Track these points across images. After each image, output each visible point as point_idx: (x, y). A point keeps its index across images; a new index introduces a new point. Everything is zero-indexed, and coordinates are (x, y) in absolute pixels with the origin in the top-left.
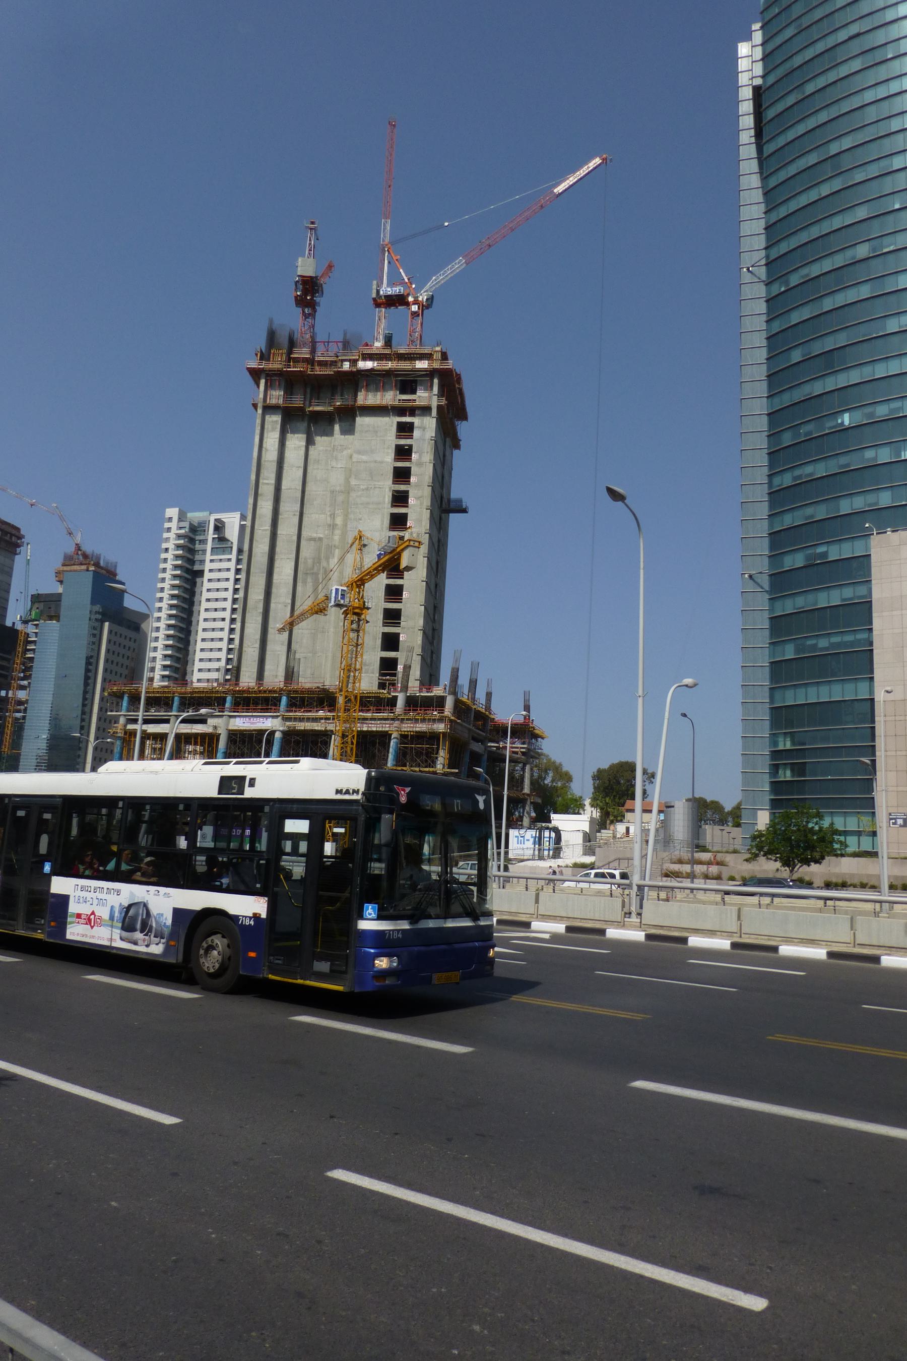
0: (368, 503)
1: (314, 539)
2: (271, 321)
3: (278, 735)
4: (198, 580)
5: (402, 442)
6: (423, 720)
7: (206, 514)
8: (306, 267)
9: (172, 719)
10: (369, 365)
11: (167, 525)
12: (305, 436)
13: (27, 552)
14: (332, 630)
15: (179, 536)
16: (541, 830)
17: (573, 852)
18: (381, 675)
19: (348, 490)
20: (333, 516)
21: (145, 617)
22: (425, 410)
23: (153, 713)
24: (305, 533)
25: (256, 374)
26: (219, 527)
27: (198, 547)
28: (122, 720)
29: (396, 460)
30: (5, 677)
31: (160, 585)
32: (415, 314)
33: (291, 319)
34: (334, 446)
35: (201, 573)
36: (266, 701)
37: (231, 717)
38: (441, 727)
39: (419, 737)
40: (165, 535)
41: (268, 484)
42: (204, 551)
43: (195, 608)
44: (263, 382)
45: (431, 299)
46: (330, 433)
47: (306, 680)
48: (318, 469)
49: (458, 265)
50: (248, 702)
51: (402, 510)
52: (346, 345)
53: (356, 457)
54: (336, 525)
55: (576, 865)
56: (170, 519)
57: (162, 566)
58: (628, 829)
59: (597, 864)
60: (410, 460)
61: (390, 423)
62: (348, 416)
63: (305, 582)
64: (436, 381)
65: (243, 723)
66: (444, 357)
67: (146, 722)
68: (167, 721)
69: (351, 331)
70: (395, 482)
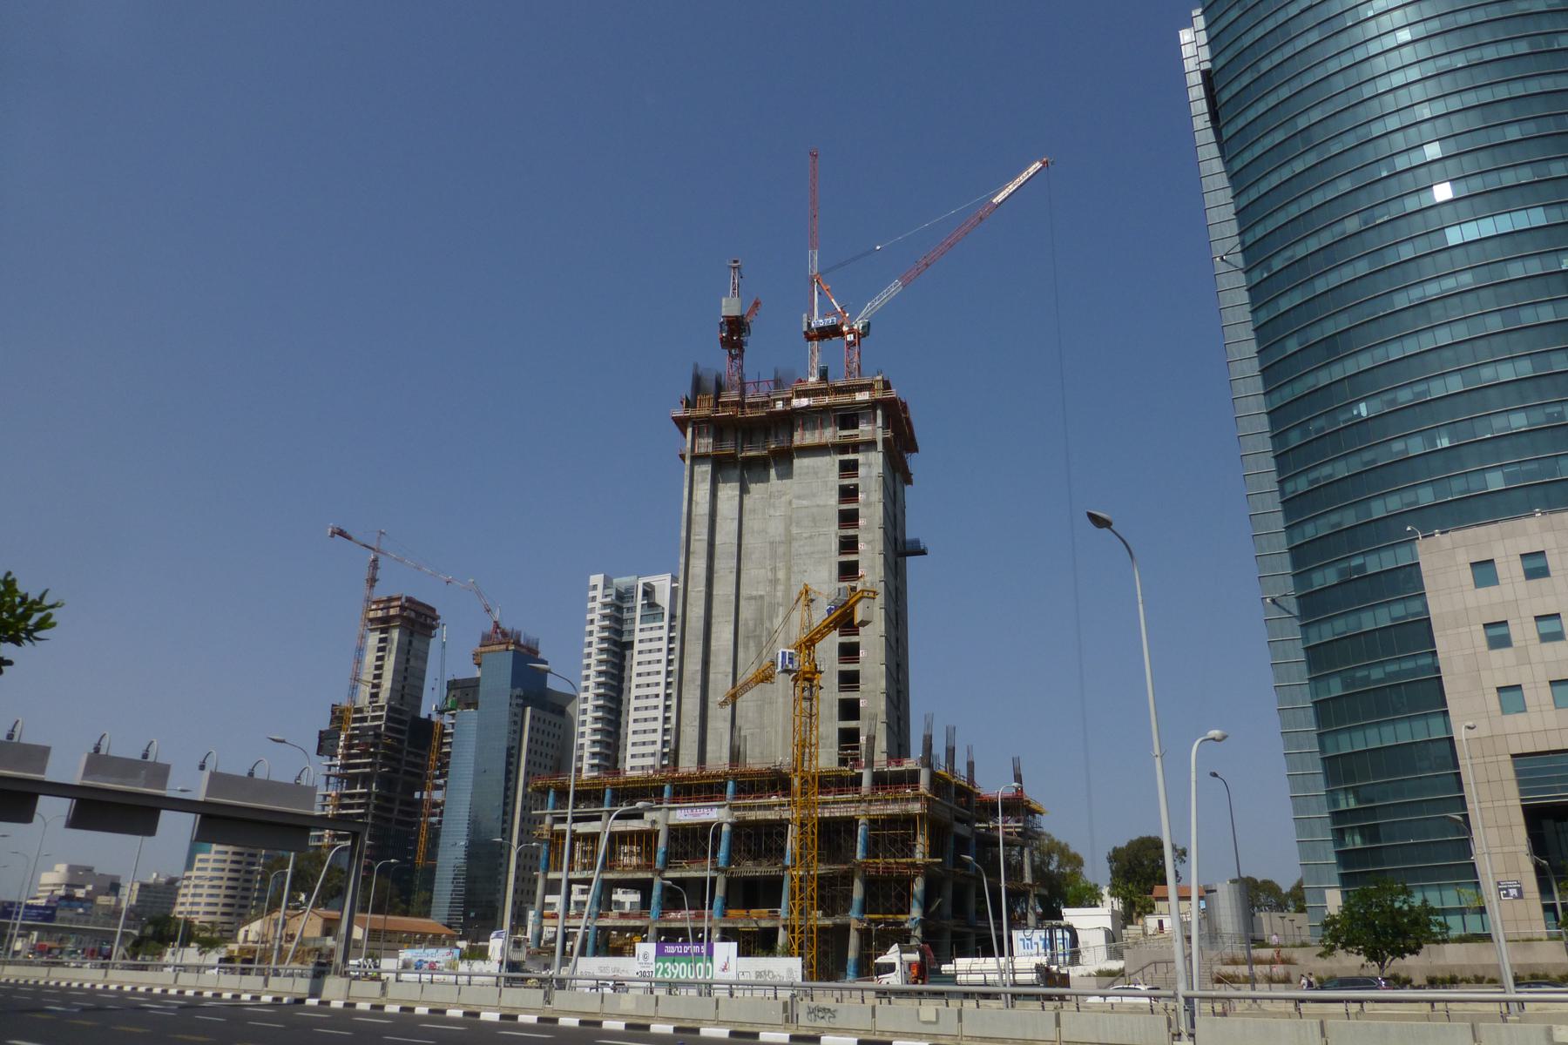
1: (754, 598)
2: (696, 366)
3: (725, 828)
4: (628, 653)
5: (847, 482)
6: (895, 801)
7: (633, 578)
8: (731, 306)
10: (804, 402)
11: (591, 594)
12: (737, 485)
13: (442, 633)
14: (781, 700)
15: (605, 605)
16: (1051, 929)
17: (1095, 957)
18: (841, 749)
19: (789, 539)
20: (774, 570)
21: (571, 698)
22: (870, 445)
23: (582, 809)
24: (743, 592)
25: (681, 423)
26: (649, 592)
27: (626, 615)
28: (548, 820)
29: (841, 502)
30: (419, 776)
31: (586, 661)
32: (851, 344)
33: (718, 362)
34: (771, 493)
35: (630, 645)
36: (710, 787)
38: (916, 808)
39: (892, 821)
40: (590, 605)
42: (633, 620)
43: (625, 685)
44: (690, 430)
45: (867, 327)
46: (766, 479)
47: (756, 760)
49: (895, 287)
50: (689, 790)
51: (852, 558)
52: (778, 383)
53: (796, 503)
55: (1100, 973)
56: (595, 587)
57: (587, 639)
58: (1161, 923)
59: (1128, 971)
60: (857, 501)
61: (832, 462)
62: (784, 458)
63: (747, 647)
64: (879, 412)
65: (685, 815)
66: (887, 386)
67: (576, 820)
68: (598, 818)
69: (784, 368)
70: (841, 527)
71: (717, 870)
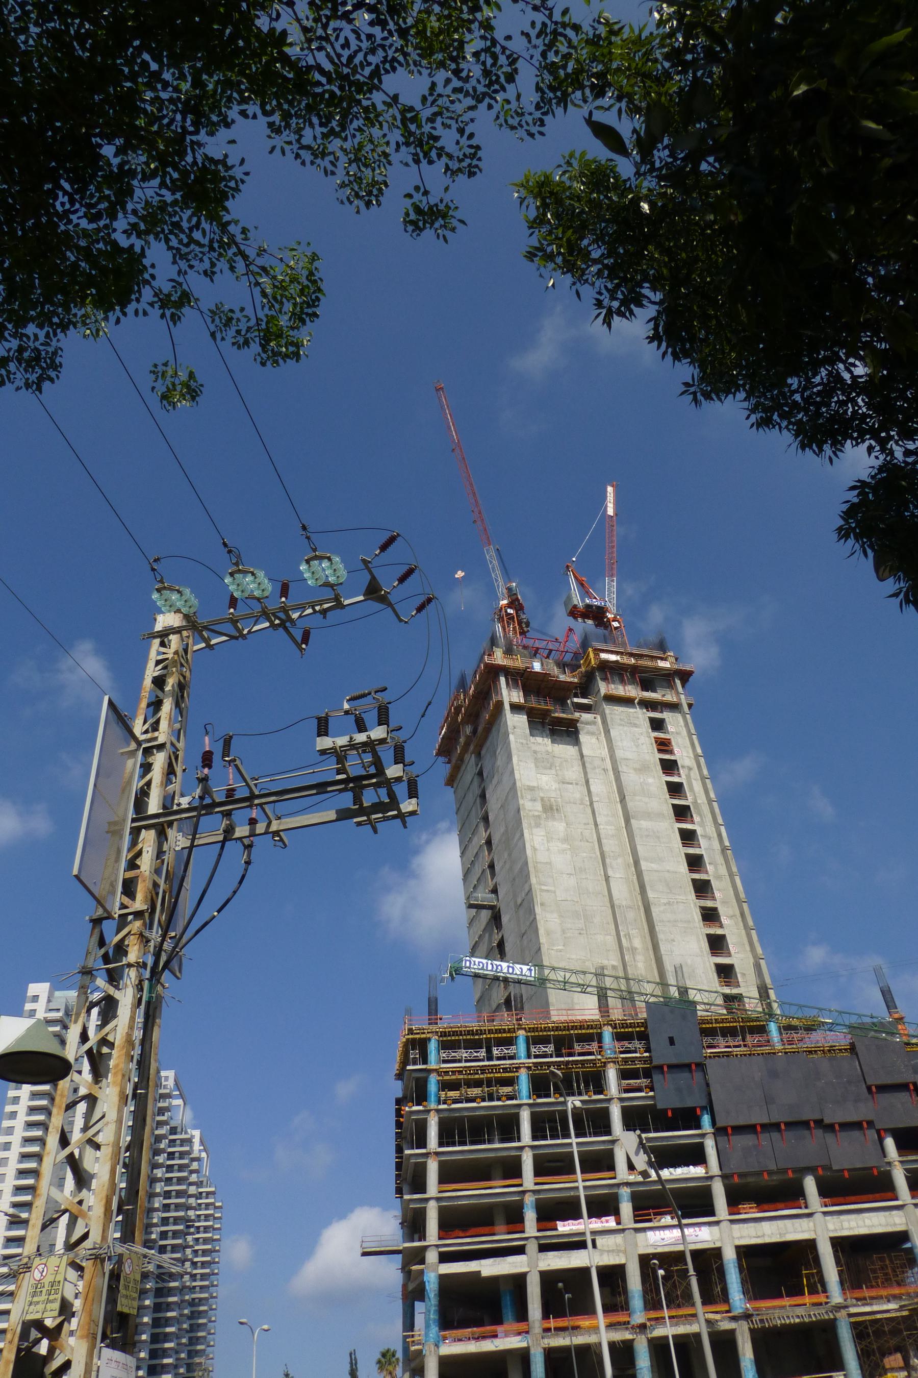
0: (676, 921)
3: (729, 1255)
9: (532, 1247)
28: (432, 1257)
37: (637, 1230)
41: (548, 891)
48: (586, 879)
54: (636, 949)
56: (35, 998)
65: (664, 1237)
68: (520, 1251)
71: (734, 1319)
